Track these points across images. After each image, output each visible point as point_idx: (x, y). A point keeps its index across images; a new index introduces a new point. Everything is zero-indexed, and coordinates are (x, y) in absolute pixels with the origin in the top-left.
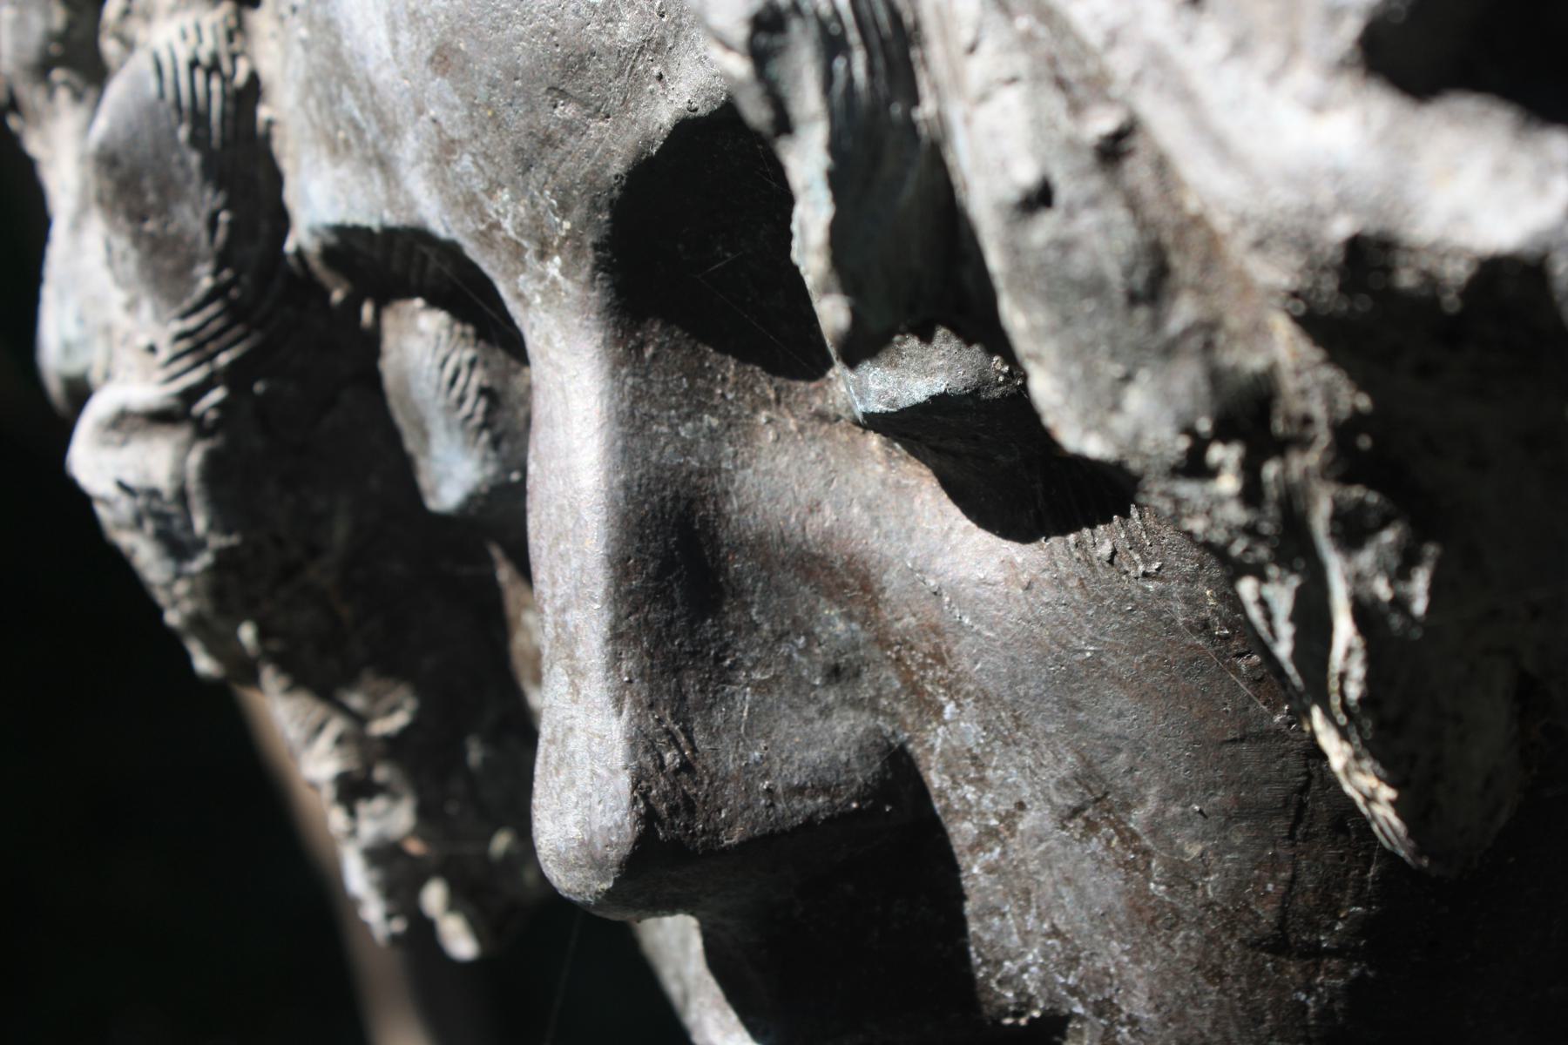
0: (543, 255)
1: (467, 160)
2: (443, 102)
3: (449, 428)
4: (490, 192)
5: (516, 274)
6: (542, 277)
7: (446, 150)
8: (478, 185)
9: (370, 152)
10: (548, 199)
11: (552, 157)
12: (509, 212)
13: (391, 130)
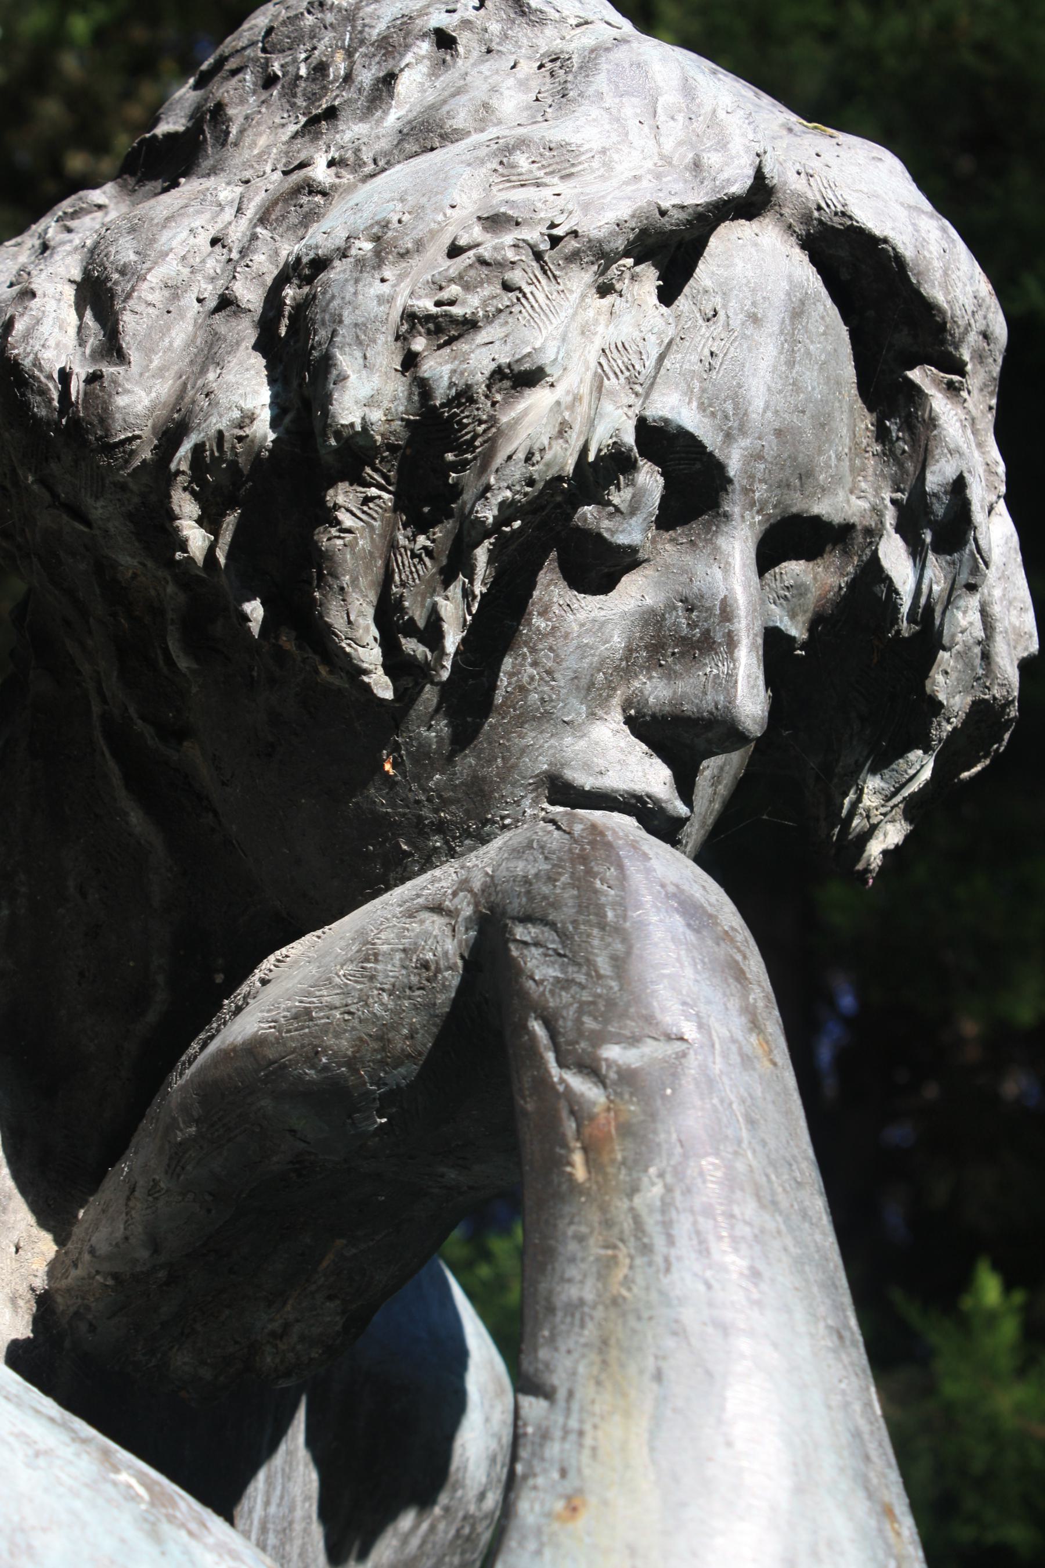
0: (758, 512)
1: (763, 466)
2: (771, 445)
3: (645, 519)
4: (760, 481)
5: (747, 510)
6: (753, 518)
7: (759, 457)
8: (759, 475)
9: (725, 428)
10: (774, 500)
11: (785, 491)
12: (761, 491)
13: (742, 430)
